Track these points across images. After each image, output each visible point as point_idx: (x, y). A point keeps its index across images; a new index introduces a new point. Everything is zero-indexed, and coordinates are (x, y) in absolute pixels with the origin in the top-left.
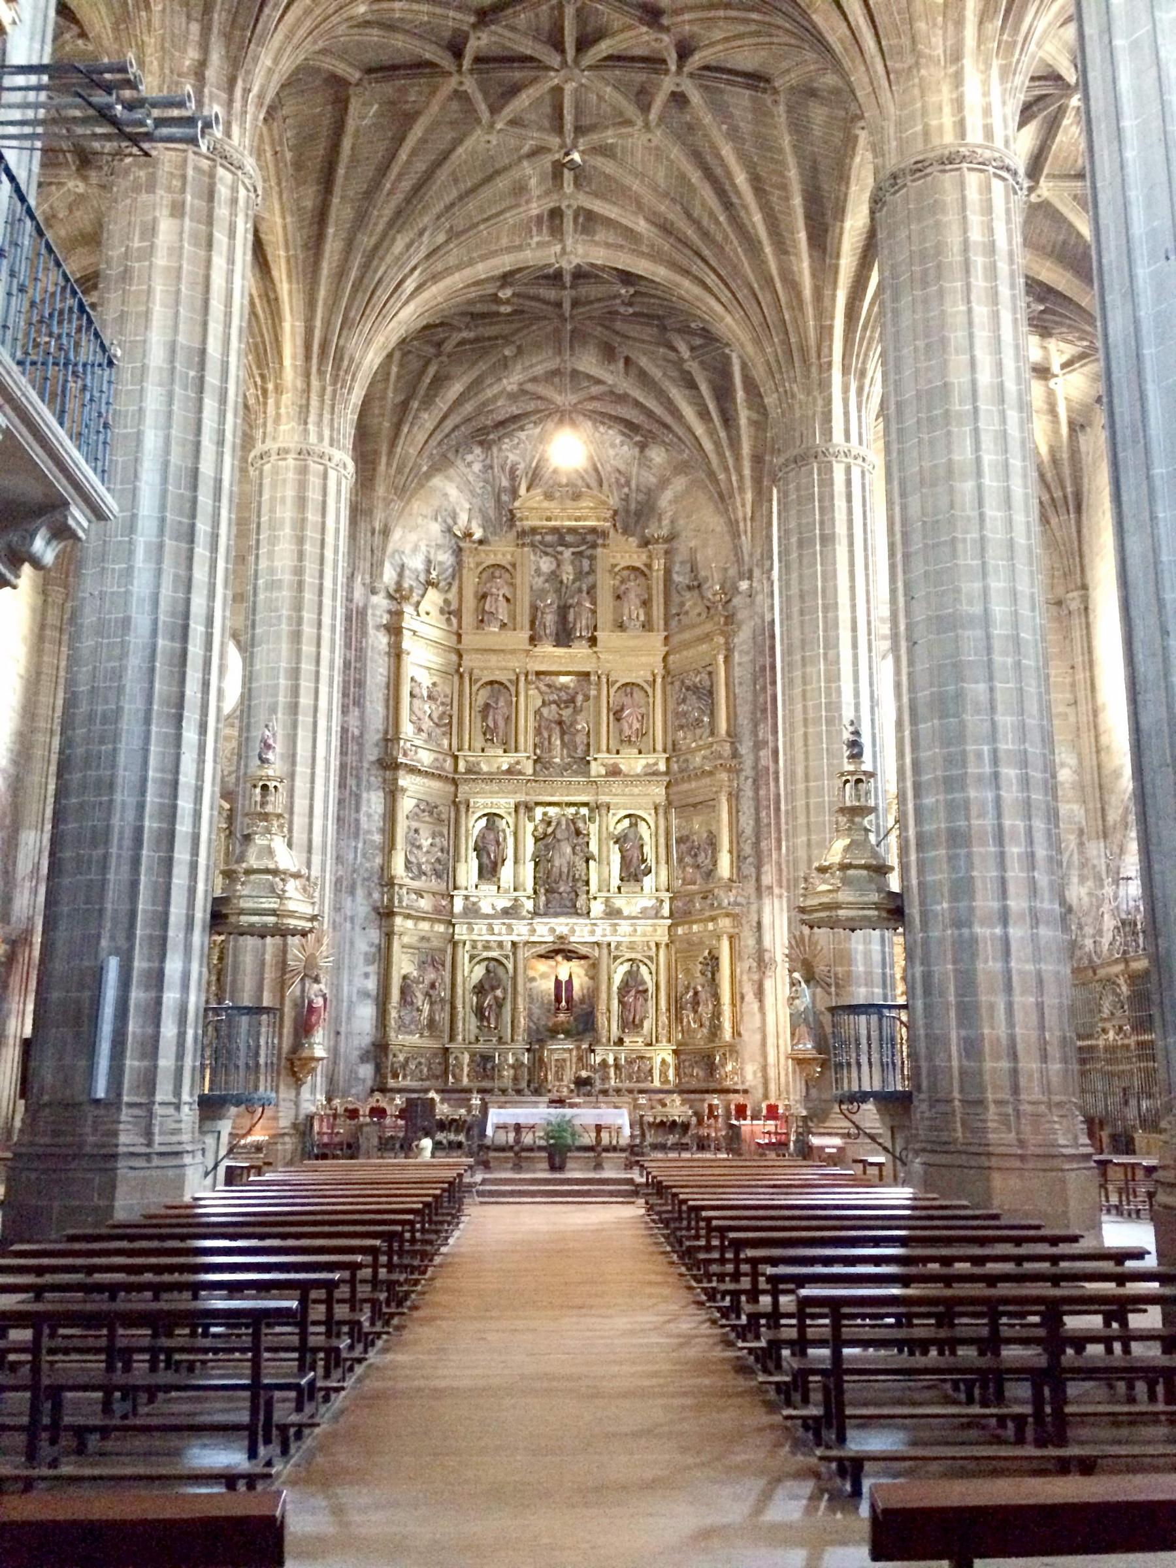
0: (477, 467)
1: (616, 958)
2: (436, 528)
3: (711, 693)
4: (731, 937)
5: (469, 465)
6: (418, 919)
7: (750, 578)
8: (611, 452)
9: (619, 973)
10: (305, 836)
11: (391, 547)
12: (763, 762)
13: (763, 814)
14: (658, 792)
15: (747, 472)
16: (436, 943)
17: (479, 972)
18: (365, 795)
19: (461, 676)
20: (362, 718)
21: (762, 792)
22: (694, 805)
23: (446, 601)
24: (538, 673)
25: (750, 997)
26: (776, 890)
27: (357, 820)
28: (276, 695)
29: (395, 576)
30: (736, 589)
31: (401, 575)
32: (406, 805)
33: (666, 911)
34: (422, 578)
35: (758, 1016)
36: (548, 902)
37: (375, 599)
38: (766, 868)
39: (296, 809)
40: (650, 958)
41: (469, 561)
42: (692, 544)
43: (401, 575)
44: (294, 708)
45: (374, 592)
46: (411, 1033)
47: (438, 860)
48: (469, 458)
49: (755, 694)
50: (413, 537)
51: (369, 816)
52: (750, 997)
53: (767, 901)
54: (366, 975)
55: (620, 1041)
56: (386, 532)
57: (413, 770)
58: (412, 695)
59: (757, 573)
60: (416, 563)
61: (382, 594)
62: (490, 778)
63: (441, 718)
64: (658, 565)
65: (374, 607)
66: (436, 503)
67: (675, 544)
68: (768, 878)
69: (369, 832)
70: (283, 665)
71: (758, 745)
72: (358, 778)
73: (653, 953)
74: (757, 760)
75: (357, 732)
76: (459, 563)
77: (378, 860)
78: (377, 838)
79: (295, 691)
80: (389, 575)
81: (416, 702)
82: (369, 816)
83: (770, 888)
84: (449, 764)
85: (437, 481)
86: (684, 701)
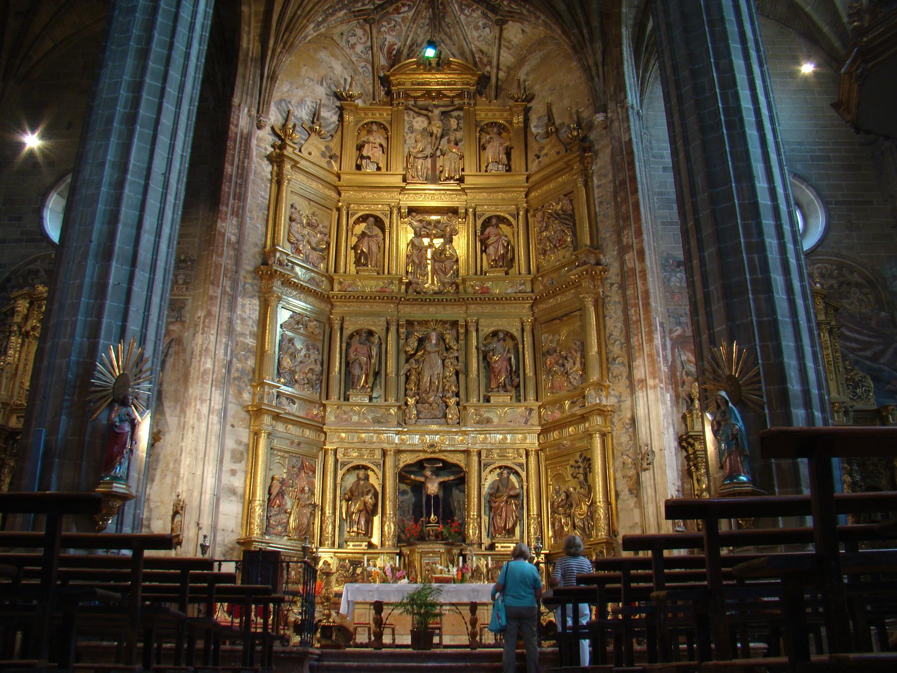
0: (359, 48)
1: (486, 465)
2: (321, 92)
3: (572, 216)
4: (603, 435)
5: (353, 47)
6: (287, 421)
7: (605, 111)
8: (476, 34)
9: (490, 479)
10: (129, 248)
11: (277, 95)
12: (629, 264)
13: (632, 311)
14: (524, 310)
15: (596, 24)
16: (304, 449)
17: (351, 480)
18: (240, 300)
19: (339, 210)
20: (241, 226)
21: (629, 292)
22: (560, 318)
23: (327, 147)
24: (412, 210)
25: (625, 493)
26: (651, 382)
27: (230, 321)
28: (114, 107)
29: (281, 121)
30: (591, 126)
31: (287, 120)
32: (283, 316)
33: (535, 419)
34: (308, 125)
35: (637, 512)
36: (419, 412)
37: (260, 133)
38: (638, 362)
39: (122, 217)
40: (521, 465)
41: (348, 118)
42: (549, 100)
43: (287, 120)
44: (131, 119)
45: (260, 127)
46: (279, 535)
47: (312, 370)
48: (353, 40)
49: (617, 206)
50: (300, 93)
51: (243, 320)
52: (625, 493)
53: (640, 394)
54: (233, 473)
55: (492, 547)
56: (273, 78)
57: (287, 282)
58: (291, 219)
59: (611, 105)
60: (303, 114)
61: (268, 128)
62: (364, 298)
63: (318, 243)
64: (518, 120)
65: (259, 140)
66: (323, 72)
67: (532, 104)
68: (640, 373)
69: (243, 335)
70: (127, 78)
71: (623, 250)
72: (235, 283)
73: (523, 460)
74: (622, 263)
75: (233, 239)
76: (341, 118)
77: (251, 362)
78: (251, 342)
79: (135, 103)
80: (274, 117)
81: (296, 227)
82: (243, 320)
83: (643, 381)
84: (325, 285)
85: (323, 55)
86: (546, 228)
